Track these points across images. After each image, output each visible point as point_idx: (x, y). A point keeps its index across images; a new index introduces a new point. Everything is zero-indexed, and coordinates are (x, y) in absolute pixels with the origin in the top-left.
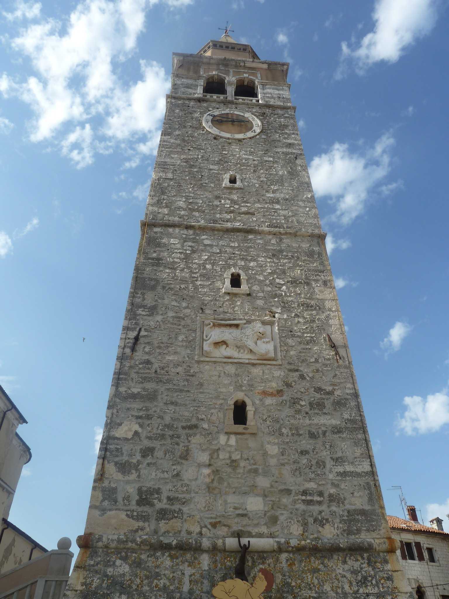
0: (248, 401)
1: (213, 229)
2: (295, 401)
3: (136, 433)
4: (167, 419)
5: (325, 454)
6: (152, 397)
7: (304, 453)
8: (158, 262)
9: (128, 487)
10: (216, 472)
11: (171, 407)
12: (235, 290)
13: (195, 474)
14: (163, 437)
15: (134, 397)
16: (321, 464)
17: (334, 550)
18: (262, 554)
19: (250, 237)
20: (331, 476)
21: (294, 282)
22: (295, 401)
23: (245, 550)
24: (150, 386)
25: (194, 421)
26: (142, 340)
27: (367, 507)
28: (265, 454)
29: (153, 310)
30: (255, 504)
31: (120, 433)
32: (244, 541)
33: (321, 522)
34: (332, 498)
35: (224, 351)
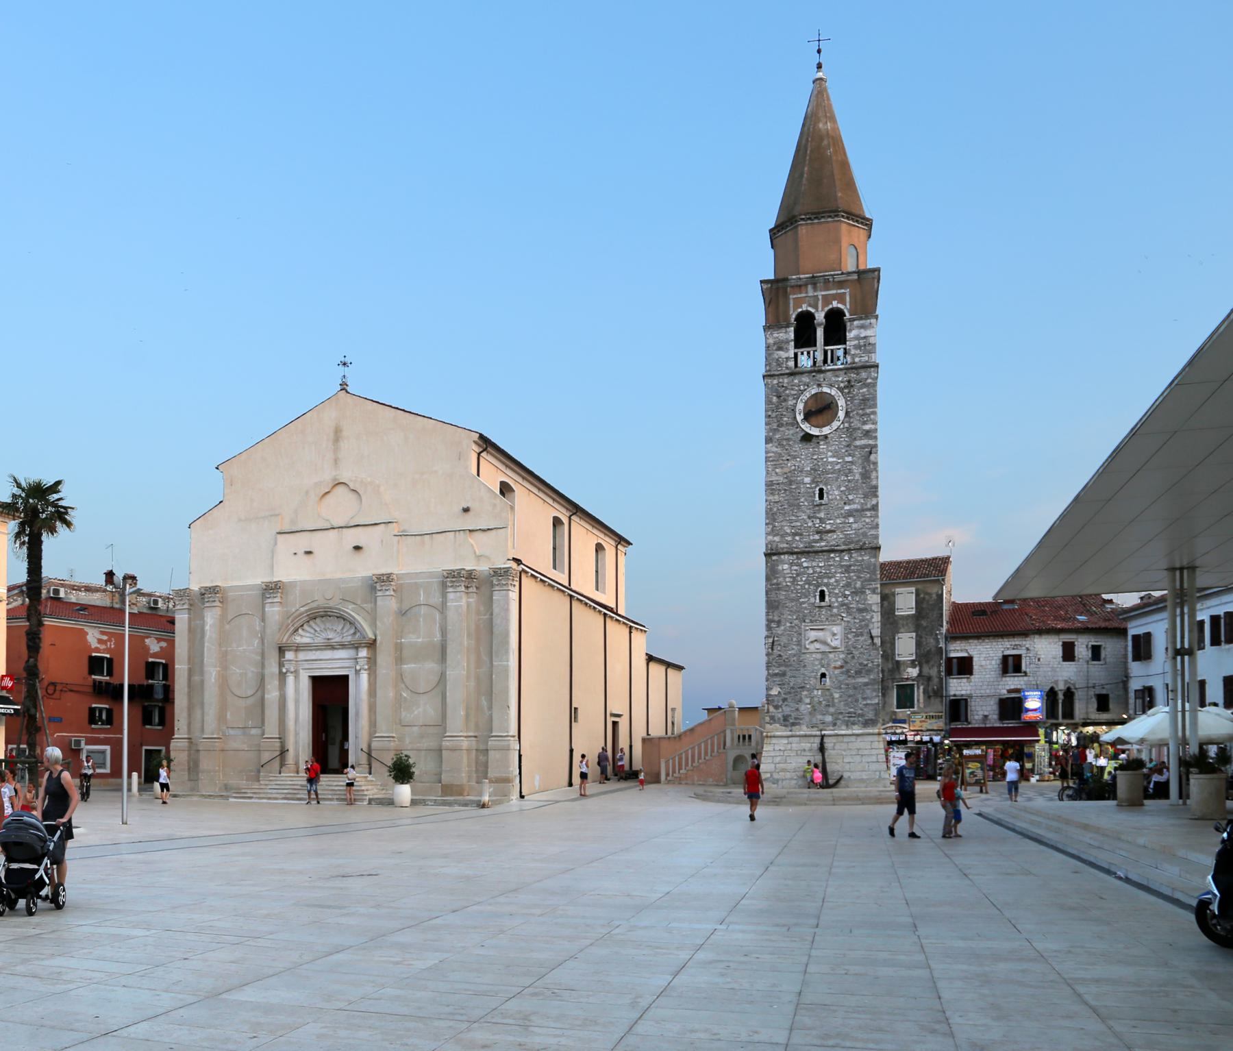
1: (808, 552)
2: (848, 671)
5: (859, 696)
6: (784, 674)
8: (778, 587)
12: (823, 604)
13: (805, 708)
15: (776, 675)
16: (857, 701)
21: (854, 593)
22: (848, 671)
23: (823, 737)
24: (783, 668)
29: (779, 623)
34: (860, 715)
35: (817, 645)
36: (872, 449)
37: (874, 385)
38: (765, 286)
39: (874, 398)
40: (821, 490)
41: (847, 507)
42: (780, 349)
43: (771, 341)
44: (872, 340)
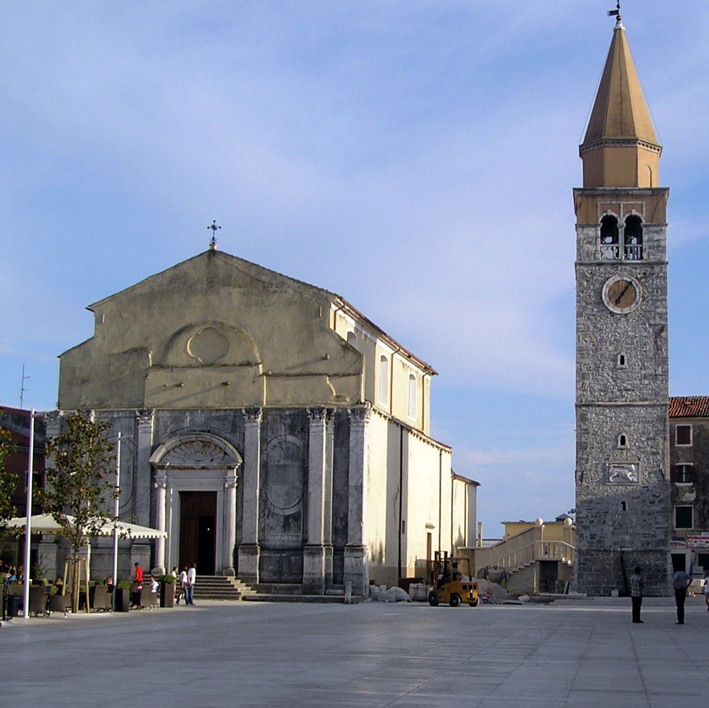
0: (626, 502)
2: (644, 501)
3: (587, 516)
4: (597, 510)
5: (652, 521)
7: (645, 521)
9: (587, 534)
10: (615, 528)
11: (599, 505)
14: (596, 516)
17: (651, 551)
18: (628, 552)
19: (631, 409)
20: (653, 529)
23: (623, 552)
25: (607, 511)
26: (584, 476)
27: (664, 538)
28: (632, 522)
30: (627, 538)
31: (581, 515)
32: (623, 549)
33: (648, 543)
34: (653, 535)
36: (663, 328)
37: (665, 278)
38: (577, 193)
39: (666, 288)
40: (622, 357)
41: (643, 372)
42: (590, 243)
43: (581, 236)
44: (662, 243)
